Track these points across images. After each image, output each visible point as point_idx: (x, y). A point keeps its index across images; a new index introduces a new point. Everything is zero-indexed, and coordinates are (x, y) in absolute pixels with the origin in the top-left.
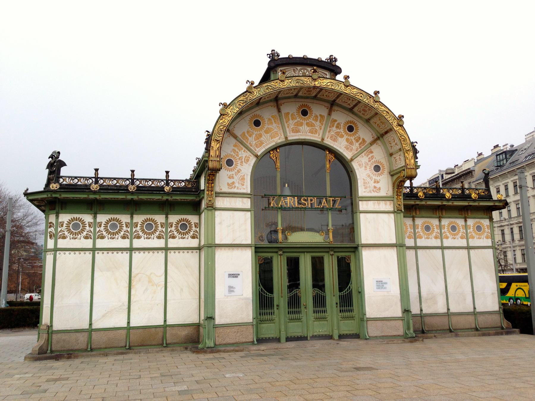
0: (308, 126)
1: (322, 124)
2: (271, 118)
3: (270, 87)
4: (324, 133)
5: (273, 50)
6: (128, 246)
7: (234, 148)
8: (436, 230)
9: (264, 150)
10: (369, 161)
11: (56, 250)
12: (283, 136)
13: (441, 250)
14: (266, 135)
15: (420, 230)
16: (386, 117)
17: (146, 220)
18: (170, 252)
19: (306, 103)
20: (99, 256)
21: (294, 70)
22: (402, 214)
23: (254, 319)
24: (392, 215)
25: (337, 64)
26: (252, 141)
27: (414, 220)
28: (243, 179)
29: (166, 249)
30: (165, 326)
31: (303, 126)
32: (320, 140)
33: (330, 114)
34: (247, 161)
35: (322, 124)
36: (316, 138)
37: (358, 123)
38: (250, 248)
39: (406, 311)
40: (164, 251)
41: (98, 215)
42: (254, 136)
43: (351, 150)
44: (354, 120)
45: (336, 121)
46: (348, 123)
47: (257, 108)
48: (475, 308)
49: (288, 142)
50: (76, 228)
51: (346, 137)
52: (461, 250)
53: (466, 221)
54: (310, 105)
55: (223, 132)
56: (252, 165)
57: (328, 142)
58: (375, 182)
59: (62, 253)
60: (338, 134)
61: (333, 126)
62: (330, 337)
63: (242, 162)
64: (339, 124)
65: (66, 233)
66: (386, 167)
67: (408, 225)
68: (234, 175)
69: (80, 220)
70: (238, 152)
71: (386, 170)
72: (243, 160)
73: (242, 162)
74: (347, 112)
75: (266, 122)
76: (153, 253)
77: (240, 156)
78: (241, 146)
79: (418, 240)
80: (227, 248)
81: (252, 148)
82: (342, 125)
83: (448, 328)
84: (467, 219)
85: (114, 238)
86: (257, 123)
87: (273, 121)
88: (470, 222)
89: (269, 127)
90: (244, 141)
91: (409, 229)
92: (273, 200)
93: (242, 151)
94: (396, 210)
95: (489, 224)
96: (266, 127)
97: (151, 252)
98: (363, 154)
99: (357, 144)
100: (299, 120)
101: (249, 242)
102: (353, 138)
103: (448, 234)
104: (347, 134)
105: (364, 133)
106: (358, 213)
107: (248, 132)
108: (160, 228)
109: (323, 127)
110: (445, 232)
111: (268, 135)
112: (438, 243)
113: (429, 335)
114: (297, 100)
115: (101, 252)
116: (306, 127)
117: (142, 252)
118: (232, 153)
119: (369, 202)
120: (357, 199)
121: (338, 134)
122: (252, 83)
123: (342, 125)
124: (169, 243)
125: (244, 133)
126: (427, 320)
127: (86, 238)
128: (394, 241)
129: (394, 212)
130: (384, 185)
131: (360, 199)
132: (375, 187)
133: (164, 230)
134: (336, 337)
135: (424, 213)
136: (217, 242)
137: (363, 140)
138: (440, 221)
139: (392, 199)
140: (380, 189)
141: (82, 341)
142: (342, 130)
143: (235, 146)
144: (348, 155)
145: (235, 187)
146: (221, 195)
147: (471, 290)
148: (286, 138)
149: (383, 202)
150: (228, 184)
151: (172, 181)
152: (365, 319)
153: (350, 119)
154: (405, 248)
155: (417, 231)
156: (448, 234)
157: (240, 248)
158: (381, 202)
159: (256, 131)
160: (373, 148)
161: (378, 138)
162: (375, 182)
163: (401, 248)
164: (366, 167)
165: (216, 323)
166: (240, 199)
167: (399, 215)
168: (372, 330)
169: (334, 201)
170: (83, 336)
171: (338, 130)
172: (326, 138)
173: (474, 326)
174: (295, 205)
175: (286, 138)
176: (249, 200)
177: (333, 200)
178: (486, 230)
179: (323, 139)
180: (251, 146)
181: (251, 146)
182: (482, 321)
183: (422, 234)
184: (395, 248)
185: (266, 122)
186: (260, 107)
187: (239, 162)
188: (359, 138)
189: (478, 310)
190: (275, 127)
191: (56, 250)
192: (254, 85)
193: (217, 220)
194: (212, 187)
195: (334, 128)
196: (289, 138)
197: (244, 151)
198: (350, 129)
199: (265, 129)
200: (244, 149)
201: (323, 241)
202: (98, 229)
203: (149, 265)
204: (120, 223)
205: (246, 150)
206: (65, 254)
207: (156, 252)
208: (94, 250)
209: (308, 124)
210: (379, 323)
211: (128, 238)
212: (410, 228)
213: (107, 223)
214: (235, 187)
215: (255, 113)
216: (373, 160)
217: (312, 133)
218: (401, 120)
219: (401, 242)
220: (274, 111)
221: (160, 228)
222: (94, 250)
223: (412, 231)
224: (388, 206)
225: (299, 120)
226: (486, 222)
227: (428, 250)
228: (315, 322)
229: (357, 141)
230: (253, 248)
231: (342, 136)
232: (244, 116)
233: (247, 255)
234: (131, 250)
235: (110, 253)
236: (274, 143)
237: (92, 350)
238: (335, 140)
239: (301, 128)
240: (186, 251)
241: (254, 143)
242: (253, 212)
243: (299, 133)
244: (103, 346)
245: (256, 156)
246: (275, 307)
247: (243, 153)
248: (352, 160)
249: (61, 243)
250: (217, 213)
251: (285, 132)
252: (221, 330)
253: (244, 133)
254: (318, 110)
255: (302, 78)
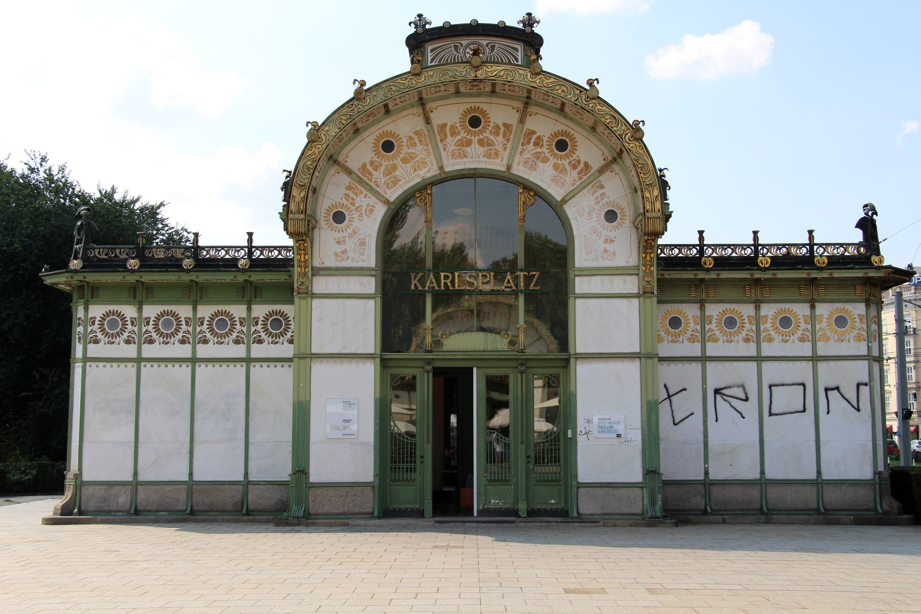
0: (483, 146)
1: (508, 140)
2: (414, 136)
3: (394, 89)
4: (511, 157)
5: (420, 16)
6: (189, 355)
7: (347, 192)
8: (747, 326)
9: (400, 191)
10: (597, 203)
11: (86, 359)
12: (435, 166)
13: (755, 363)
14: (403, 165)
15: (713, 326)
16: (609, 126)
17: (217, 314)
18: (254, 366)
19: (477, 105)
20: (147, 370)
21: (456, 48)
22: (655, 299)
23: (375, 476)
24: (635, 302)
25: (537, 29)
26: (379, 176)
27: (702, 308)
28: (363, 244)
29: (194, 361)
30: (247, 483)
31: (472, 146)
32: (504, 169)
33: (522, 121)
34: (371, 210)
35: (508, 140)
36: (498, 165)
37: (576, 135)
38: (372, 360)
39: (651, 472)
40: (244, 364)
41: (145, 307)
42: (382, 168)
43: (563, 185)
44: (569, 130)
45: (534, 133)
46: (556, 135)
47: (388, 121)
48: (819, 472)
49: (443, 175)
50: (113, 327)
51: (552, 161)
52: (798, 363)
53: (813, 307)
54: (484, 107)
55: (312, 171)
56: (379, 218)
57: (519, 170)
58: (606, 241)
59: (94, 364)
60: (537, 156)
61: (529, 143)
62: (515, 513)
63: (361, 215)
64: (539, 138)
65: (99, 335)
66: (627, 213)
67: (690, 317)
68: (347, 238)
69: (119, 314)
70: (353, 199)
71: (628, 218)
72: (363, 212)
73: (361, 215)
74: (555, 116)
75: (405, 143)
76: (228, 366)
77: (357, 205)
78: (360, 188)
79: (709, 345)
80: (331, 361)
81: (378, 189)
82: (545, 139)
83: (759, 506)
84: (817, 305)
85: (168, 343)
86: (388, 147)
87: (417, 140)
88: (823, 309)
89: (410, 151)
90: (365, 179)
91: (692, 325)
92: (415, 277)
93: (362, 196)
94: (641, 293)
95: (864, 313)
96: (404, 152)
97: (224, 365)
98: (585, 191)
99: (575, 173)
100: (465, 135)
101: (371, 350)
102: (566, 162)
103: (773, 333)
104: (555, 156)
105: (589, 151)
106: (571, 300)
107: (372, 163)
108: (238, 327)
109: (509, 146)
110: (766, 330)
111: (409, 165)
112: (695, 350)
113: (712, 517)
114: (460, 100)
115: (149, 365)
116: (477, 146)
117: (210, 365)
118: (344, 201)
119: (594, 278)
120: (571, 275)
121: (537, 156)
122: (363, 83)
123: (545, 139)
124: (252, 350)
125: (364, 165)
126: (717, 492)
127: (128, 342)
128: (636, 349)
129: (637, 296)
130: (623, 248)
131: (576, 273)
132: (606, 251)
133: (244, 329)
134: (523, 513)
135: (723, 293)
136: (315, 350)
137: (586, 164)
138: (757, 308)
139: (636, 272)
140: (614, 254)
141: (123, 499)
142: (545, 150)
143: (349, 188)
144: (557, 194)
145: (348, 258)
146: (321, 273)
147: (813, 438)
148: (441, 168)
149: (620, 277)
150: (336, 254)
151: (257, 248)
152: (574, 483)
153: (559, 127)
154: (657, 359)
155: (707, 327)
156: (773, 333)
157: (354, 361)
158: (616, 277)
159: (386, 161)
160: (605, 178)
161: (614, 160)
162: (606, 241)
163: (649, 361)
164: (590, 214)
165: (311, 481)
166: (357, 278)
167: (648, 301)
168: (586, 505)
169: (528, 279)
170: (125, 492)
171: (539, 150)
172: (515, 165)
173: (813, 505)
174: (453, 286)
175: (441, 168)
176: (373, 279)
177: (525, 276)
178: (858, 324)
179: (509, 168)
180: (378, 186)
181: (378, 186)
182: (832, 497)
183: (717, 333)
184: (638, 361)
185: (405, 143)
186: (393, 118)
187: (356, 215)
188: (579, 162)
189: (825, 476)
190: (419, 150)
191: (86, 359)
192: (365, 88)
193: (315, 315)
194: (306, 261)
195: (531, 147)
196: (447, 169)
197: (365, 197)
198: (562, 146)
199: (402, 156)
200: (365, 192)
201: (506, 348)
202: (144, 329)
203: (220, 384)
204: (177, 318)
205: (369, 195)
206: (97, 366)
207: (231, 365)
208: (139, 360)
209: (481, 143)
210: (600, 492)
211: (189, 343)
212: (695, 322)
213: (158, 319)
214: (348, 258)
215: (385, 129)
216: (604, 202)
217: (489, 157)
218: (639, 130)
219: (649, 350)
220: (418, 123)
221: (238, 327)
222: (139, 360)
223: (699, 327)
224: (630, 285)
225: (465, 135)
226: (857, 309)
227: (727, 364)
228: (488, 487)
229: (574, 167)
230: (378, 360)
231: (545, 160)
232: (364, 135)
233: (368, 372)
234: (194, 361)
235: (163, 365)
236: (419, 180)
237: (137, 512)
238: (533, 168)
239: (468, 149)
240: (279, 364)
241: (383, 180)
242: (379, 300)
243: (466, 159)
244: (154, 507)
245: (387, 202)
246: (418, 459)
247: (364, 200)
248: (564, 201)
249: (94, 350)
250: (316, 302)
251: (439, 159)
252: (319, 491)
253: (364, 165)
254: (500, 113)
255: (453, 67)
